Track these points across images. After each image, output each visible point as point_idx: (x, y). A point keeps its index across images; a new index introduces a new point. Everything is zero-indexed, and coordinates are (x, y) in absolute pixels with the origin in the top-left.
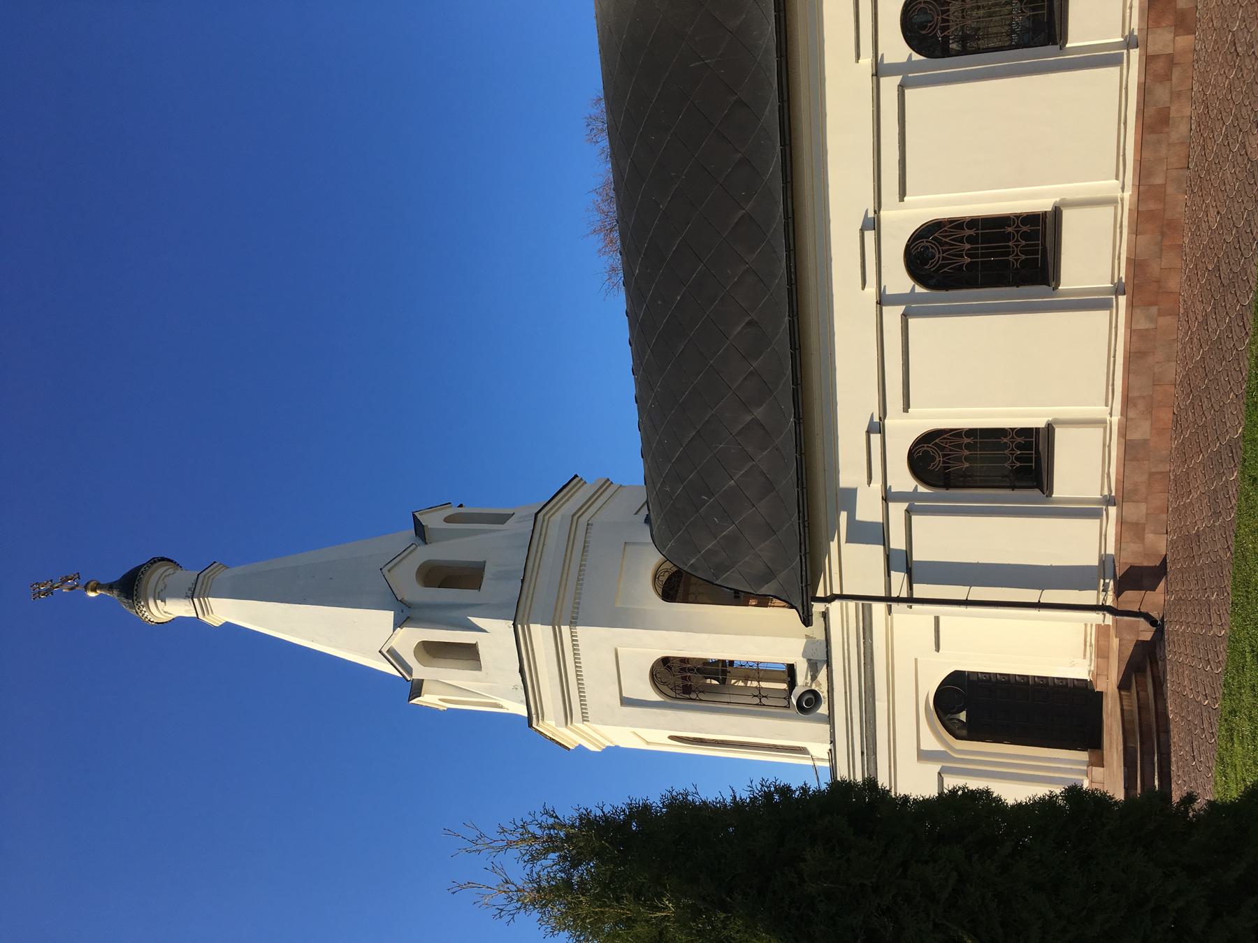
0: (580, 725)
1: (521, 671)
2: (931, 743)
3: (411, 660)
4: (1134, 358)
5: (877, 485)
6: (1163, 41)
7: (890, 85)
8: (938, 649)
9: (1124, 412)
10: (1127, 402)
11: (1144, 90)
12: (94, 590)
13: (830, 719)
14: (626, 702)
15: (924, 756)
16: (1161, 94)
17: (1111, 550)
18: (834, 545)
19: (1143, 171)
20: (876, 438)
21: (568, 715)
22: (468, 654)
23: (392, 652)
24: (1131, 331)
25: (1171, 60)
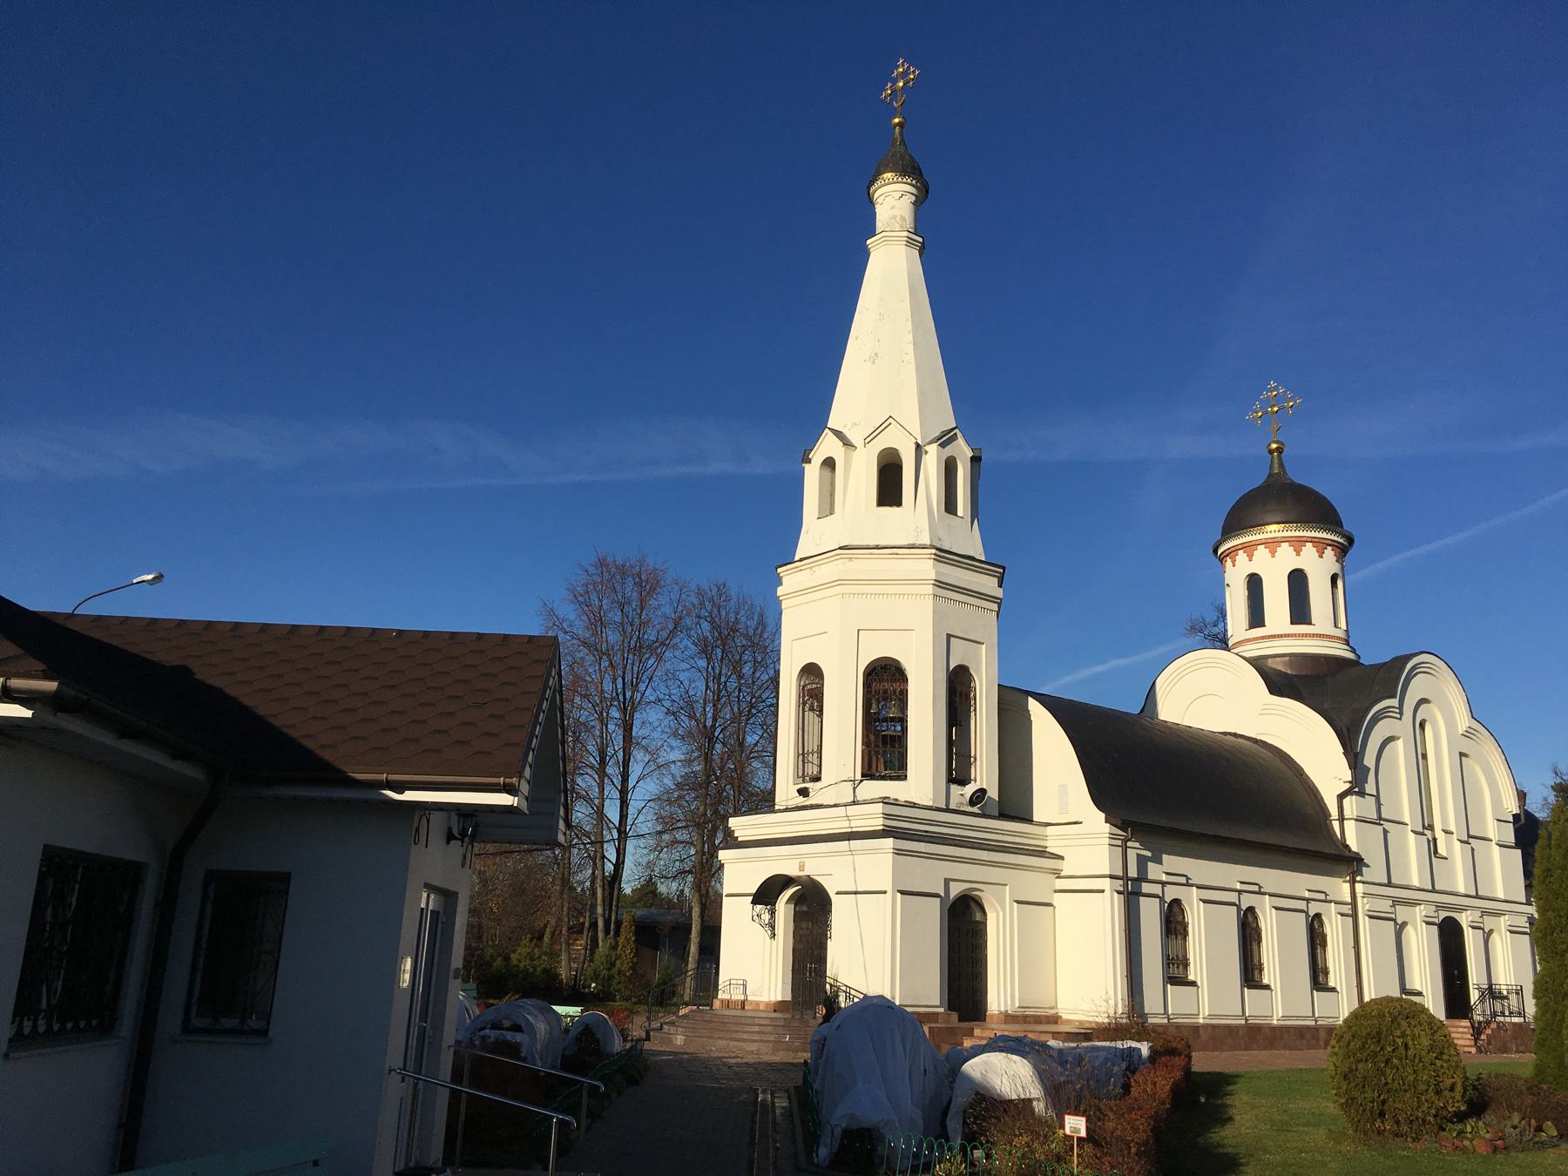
0: (930, 589)
1: (973, 559)
2: (956, 890)
3: (949, 451)
4: (1228, 1027)
5: (1164, 878)
6: (1323, 1034)
7: (1301, 905)
8: (1018, 902)
9: (1205, 1026)
10: (1214, 1027)
11: (1308, 1028)
12: (899, 124)
13: (948, 810)
14: (949, 636)
15: (947, 881)
16: (1309, 1036)
17: (1150, 1021)
18: (1137, 845)
19: (1287, 1028)
20: (1183, 880)
21: (940, 584)
22: (950, 506)
23: (954, 438)
24: (1238, 1027)
25: (1317, 1039)
